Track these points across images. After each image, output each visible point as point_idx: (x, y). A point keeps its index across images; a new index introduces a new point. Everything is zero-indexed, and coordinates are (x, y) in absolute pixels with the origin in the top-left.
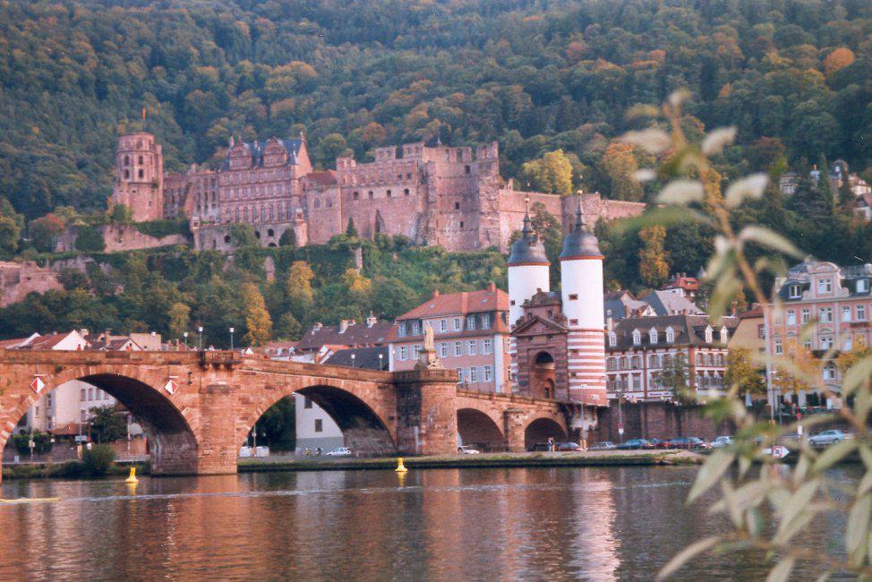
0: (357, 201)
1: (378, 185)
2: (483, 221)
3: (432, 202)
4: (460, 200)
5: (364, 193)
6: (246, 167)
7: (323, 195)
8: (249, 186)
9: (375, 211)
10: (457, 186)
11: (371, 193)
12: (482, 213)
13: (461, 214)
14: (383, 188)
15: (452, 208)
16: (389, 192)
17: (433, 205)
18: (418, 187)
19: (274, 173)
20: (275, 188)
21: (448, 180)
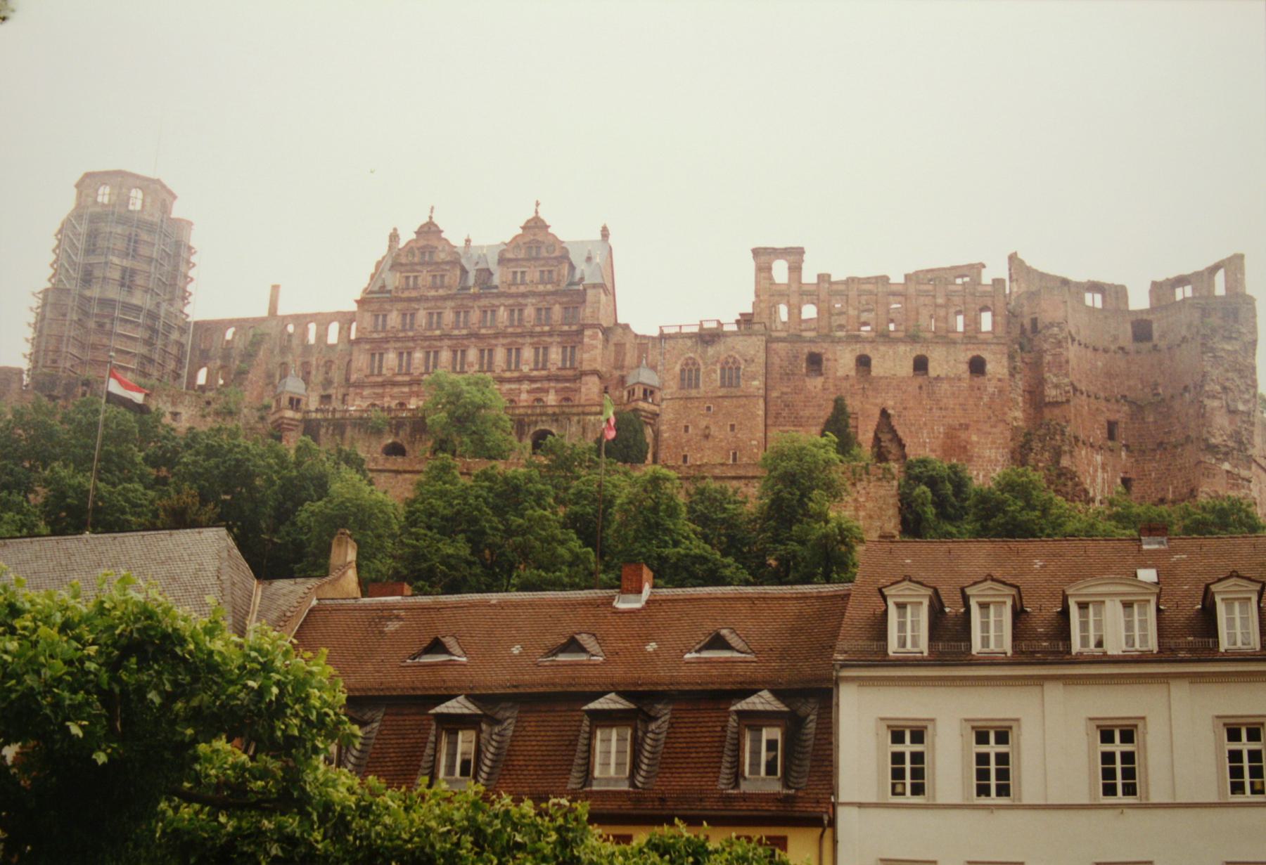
0: (819, 381)
1: (884, 337)
2: (1209, 473)
3: (1056, 404)
4: (1121, 414)
5: (843, 361)
6: (441, 292)
7: (711, 351)
8: (447, 342)
9: (877, 413)
10: (1109, 375)
11: (864, 362)
12: (1212, 449)
13: (1123, 454)
14: (902, 348)
15: (1099, 434)
16: (921, 365)
17: (1057, 411)
18: (1011, 357)
19: (529, 312)
20: (528, 353)
21: (1090, 354)
